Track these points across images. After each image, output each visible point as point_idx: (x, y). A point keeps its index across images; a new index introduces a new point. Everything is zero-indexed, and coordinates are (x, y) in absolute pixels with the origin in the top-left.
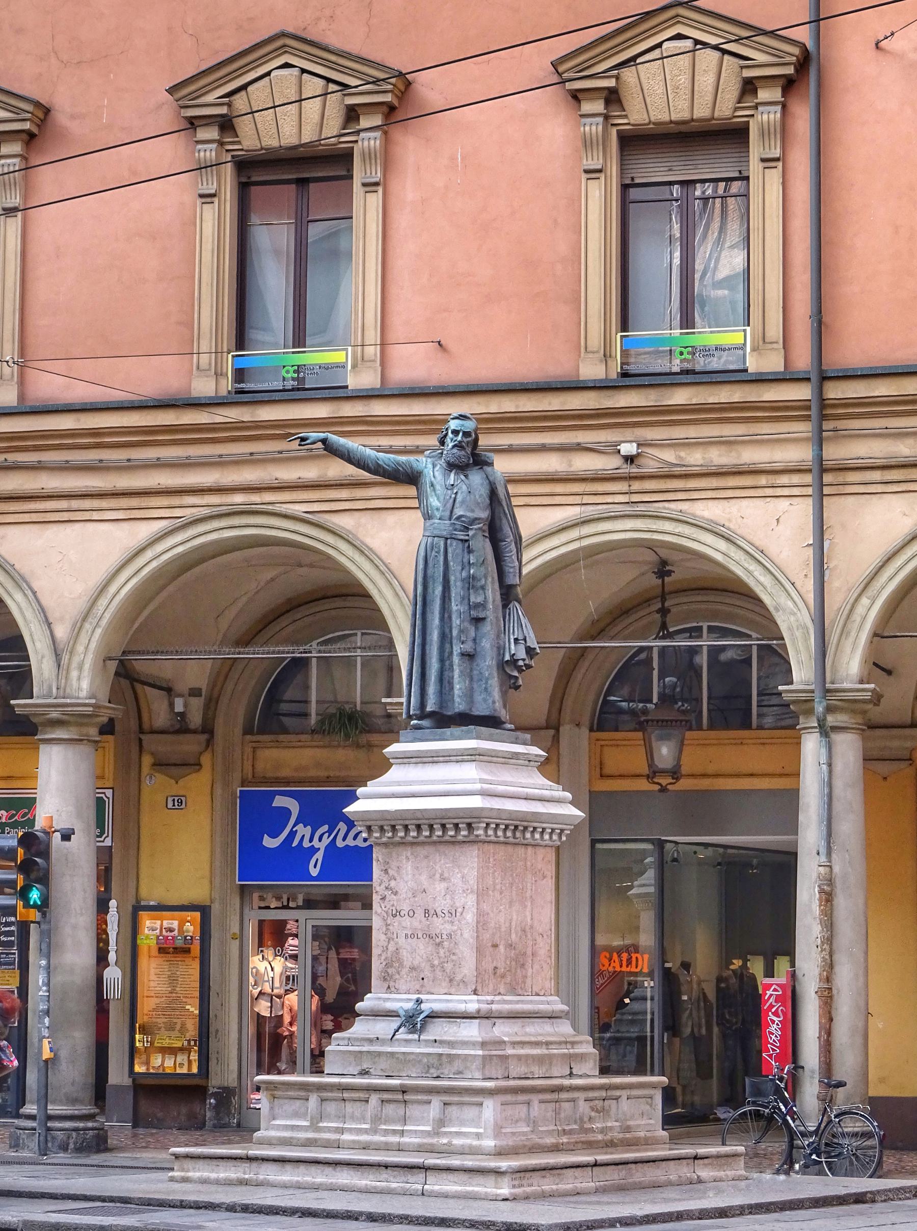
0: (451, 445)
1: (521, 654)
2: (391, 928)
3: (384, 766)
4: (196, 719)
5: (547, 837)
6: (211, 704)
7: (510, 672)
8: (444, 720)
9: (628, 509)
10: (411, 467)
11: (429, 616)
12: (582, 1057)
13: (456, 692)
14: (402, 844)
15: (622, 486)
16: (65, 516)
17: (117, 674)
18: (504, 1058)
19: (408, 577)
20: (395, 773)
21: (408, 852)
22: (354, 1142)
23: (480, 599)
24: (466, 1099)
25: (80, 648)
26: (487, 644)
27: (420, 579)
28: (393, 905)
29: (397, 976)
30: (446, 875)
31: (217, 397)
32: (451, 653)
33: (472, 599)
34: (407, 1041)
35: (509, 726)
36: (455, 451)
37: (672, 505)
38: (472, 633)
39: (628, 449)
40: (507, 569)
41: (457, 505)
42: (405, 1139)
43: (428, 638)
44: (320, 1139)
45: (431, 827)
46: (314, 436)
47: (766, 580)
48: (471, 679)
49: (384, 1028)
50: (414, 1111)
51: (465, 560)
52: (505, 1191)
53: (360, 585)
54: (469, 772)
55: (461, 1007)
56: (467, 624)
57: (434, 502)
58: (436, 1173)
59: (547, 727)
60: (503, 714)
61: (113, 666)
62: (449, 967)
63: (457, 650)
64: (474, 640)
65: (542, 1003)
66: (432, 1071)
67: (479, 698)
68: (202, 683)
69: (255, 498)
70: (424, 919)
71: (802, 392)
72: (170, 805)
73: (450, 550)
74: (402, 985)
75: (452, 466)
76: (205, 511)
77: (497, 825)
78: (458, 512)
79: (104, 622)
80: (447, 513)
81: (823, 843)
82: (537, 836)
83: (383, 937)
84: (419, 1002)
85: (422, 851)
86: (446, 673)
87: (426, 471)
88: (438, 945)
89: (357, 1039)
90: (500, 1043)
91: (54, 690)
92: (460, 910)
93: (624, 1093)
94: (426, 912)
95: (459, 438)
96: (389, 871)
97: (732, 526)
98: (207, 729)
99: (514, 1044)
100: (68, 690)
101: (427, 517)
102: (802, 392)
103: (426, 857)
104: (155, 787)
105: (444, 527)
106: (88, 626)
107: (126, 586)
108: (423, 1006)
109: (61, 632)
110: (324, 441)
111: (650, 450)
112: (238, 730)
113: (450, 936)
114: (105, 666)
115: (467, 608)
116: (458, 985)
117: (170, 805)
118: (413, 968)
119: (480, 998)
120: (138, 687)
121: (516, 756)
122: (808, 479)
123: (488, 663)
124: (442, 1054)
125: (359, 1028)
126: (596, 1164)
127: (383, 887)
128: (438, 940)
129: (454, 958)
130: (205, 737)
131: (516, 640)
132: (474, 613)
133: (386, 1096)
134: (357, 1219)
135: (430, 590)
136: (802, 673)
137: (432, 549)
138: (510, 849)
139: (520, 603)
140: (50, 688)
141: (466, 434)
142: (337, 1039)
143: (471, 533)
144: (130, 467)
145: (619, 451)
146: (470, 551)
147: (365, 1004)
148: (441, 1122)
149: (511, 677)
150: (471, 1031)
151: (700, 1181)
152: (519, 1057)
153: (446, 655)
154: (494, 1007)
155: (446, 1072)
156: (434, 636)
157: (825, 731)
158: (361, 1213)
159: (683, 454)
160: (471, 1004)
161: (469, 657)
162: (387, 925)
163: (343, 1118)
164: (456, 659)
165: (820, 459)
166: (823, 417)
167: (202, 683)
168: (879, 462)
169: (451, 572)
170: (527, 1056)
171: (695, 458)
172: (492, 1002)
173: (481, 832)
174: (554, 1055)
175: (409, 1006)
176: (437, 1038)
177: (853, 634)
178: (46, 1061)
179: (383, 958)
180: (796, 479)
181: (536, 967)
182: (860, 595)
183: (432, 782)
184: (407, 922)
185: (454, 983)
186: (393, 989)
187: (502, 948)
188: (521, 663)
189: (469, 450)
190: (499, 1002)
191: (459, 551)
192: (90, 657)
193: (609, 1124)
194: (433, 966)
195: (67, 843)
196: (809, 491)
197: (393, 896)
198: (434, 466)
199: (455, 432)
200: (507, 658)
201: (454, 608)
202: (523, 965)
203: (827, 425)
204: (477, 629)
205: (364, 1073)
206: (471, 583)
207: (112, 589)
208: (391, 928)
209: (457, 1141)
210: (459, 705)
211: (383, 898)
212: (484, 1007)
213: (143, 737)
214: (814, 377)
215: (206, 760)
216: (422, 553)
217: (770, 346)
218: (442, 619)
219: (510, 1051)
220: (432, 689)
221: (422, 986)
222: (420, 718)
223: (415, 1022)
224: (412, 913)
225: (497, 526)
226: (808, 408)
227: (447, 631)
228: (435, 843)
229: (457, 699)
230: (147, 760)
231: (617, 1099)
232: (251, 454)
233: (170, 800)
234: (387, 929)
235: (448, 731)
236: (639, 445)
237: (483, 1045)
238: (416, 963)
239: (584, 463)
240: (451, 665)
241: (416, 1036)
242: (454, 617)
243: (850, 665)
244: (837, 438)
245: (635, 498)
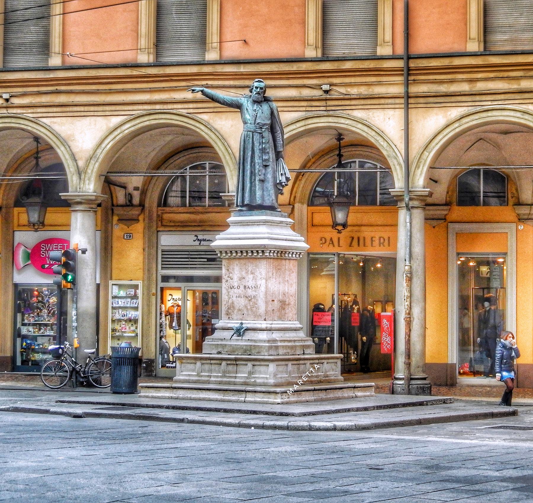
0: (255, 93)
1: (284, 180)
3: (227, 226)
4: (136, 200)
5: (294, 256)
6: (144, 193)
7: (278, 187)
8: (252, 208)
9: (325, 113)
10: (238, 102)
11: (246, 164)
12: (308, 347)
13: (257, 196)
14: (235, 258)
15: (323, 103)
16: (83, 114)
17: (104, 181)
18: (277, 347)
19: (235, 145)
20: (231, 230)
21: (237, 262)
22: (215, 381)
23: (267, 157)
24: (262, 363)
25: (89, 171)
26: (270, 176)
27: (242, 149)
30: (253, 272)
31: (148, 63)
32: (255, 179)
33: (264, 158)
34: (238, 340)
35: (279, 210)
36: (256, 95)
37: (345, 112)
38: (264, 171)
39: (326, 87)
40: (278, 145)
41: (257, 118)
42: (237, 380)
43: (245, 174)
45: (247, 252)
46: (198, 89)
47: (385, 145)
48: (263, 191)
49: (227, 334)
50: (241, 368)
51: (261, 141)
52: (279, 401)
53: (207, 142)
54: (263, 229)
55: (259, 326)
56: (261, 168)
57: (248, 117)
59: (289, 204)
60: (276, 205)
61: (103, 178)
62: (254, 309)
63: (257, 178)
64: (264, 175)
65: (292, 324)
66: (248, 352)
67: (266, 198)
68: (140, 185)
69: (165, 107)
70: (244, 290)
71: (400, 64)
72: (125, 238)
73: (255, 137)
74: (234, 316)
75: (255, 102)
76: (144, 112)
77: (274, 251)
78: (258, 121)
79: (100, 160)
80: (253, 122)
81: (407, 256)
82: (290, 255)
83: (227, 297)
84: (242, 324)
86: (253, 188)
87: (244, 104)
89: (216, 339)
90: (275, 341)
91: (78, 189)
92: (259, 286)
93: (325, 361)
94: (245, 287)
95: (258, 90)
97: (370, 121)
98: (142, 205)
99: (281, 341)
100: (84, 189)
101: (245, 123)
102: (400, 64)
103: (245, 264)
104: (118, 230)
105: (252, 127)
106: (92, 162)
107: (108, 144)
108: (244, 325)
109: (81, 163)
110: (202, 91)
111: (334, 88)
112: (155, 204)
113: (254, 297)
114: (100, 178)
115: (261, 161)
117: (125, 238)
118: (239, 310)
119: (267, 322)
120: (112, 187)
121: (281, 222)
122: (402, 101)
123: (270, 185)
125: (217, 334)
126: (315, 390)
130: (141, 208)
131: (282, 174)
132: (265, 163)
133: (229, 362)
135: (246, 153)
136: (399, 184)
137: (247, 136)
138: (279, 260)
139: (283, 159)
140: (76, 188)
141: (261, 88)
142: (207, 339)
143: (263, 130)
144: (110, 92)
145: (322, 88)
146: (263, 137)
147: (219, 323)
148: (250, 373)
149: (279, 189)
150: (263, 336)
151: (356, 397)
152: (283, 346)
153: (253, 180)
154: (273, 326)
155: (253, 352)
156: (248, 173)
157: (409, 208)
158: (221, 409)
159: (349, 90)
160: (264, 325)
161: (262, 181)
164: (257, 183)
165: (407, 92)
166: (409, 75)
167: (140, 185)
168: (432, 94)
169: (255, 146)
170: (286, 346)
171: (354, 91)
172: (272, 324)
173: (268, 254)
174: (297, 346)
175: (237, 325)
177: (421, 167)
178: (76, 348)
180: (398, 101)
181: (290, 309)
182: (424, 151)
184: (236, 290)
185: (257, 316)
187: (276, 301)
188: (283, 184)
189: (262, 95)
190: (275, 324)
191: (258, 137)
192: (94, 174)
193: (319, 374)
194: (247, 309)
195: (84, 255)
196: (403, 106)
198: (248, 101)
199: (257, 88)
200: (278, 182)
201: (257, 161)
202: (284, 309)
203: (411, 78)
204: (265, 170)
205: (219, 353)
206: (263, 151)
207: (103, 145)
209: (258, 381)
210: (259, 201)
211: (227, 281)
212: (269, 326)
213: (113, 208)
214: (405, 58)
215: (141, 218)
216: (243, 138)
217: (387, 44)
218: (251, 166)
219: (279, 344)
220: (247, 195)
222: (242, 206)
223: (240, 332)
225: (274, 126)
226: (403, 71)
227: (253, 170)
228: (248, 258)
229: (258, 199)
230: (115, 218)
231: (322, 363)
232: (164, 88)
233: (125, 235)
235: (254, 212)
236: (330, 85)
237: (269, 341)
238: (240, 308)
239: (306, 93)
240: (255, 185)
241: (240, 338)
242: (256, 165)
243: (420, 181)
244: (414, 83)
245: (328, 108)
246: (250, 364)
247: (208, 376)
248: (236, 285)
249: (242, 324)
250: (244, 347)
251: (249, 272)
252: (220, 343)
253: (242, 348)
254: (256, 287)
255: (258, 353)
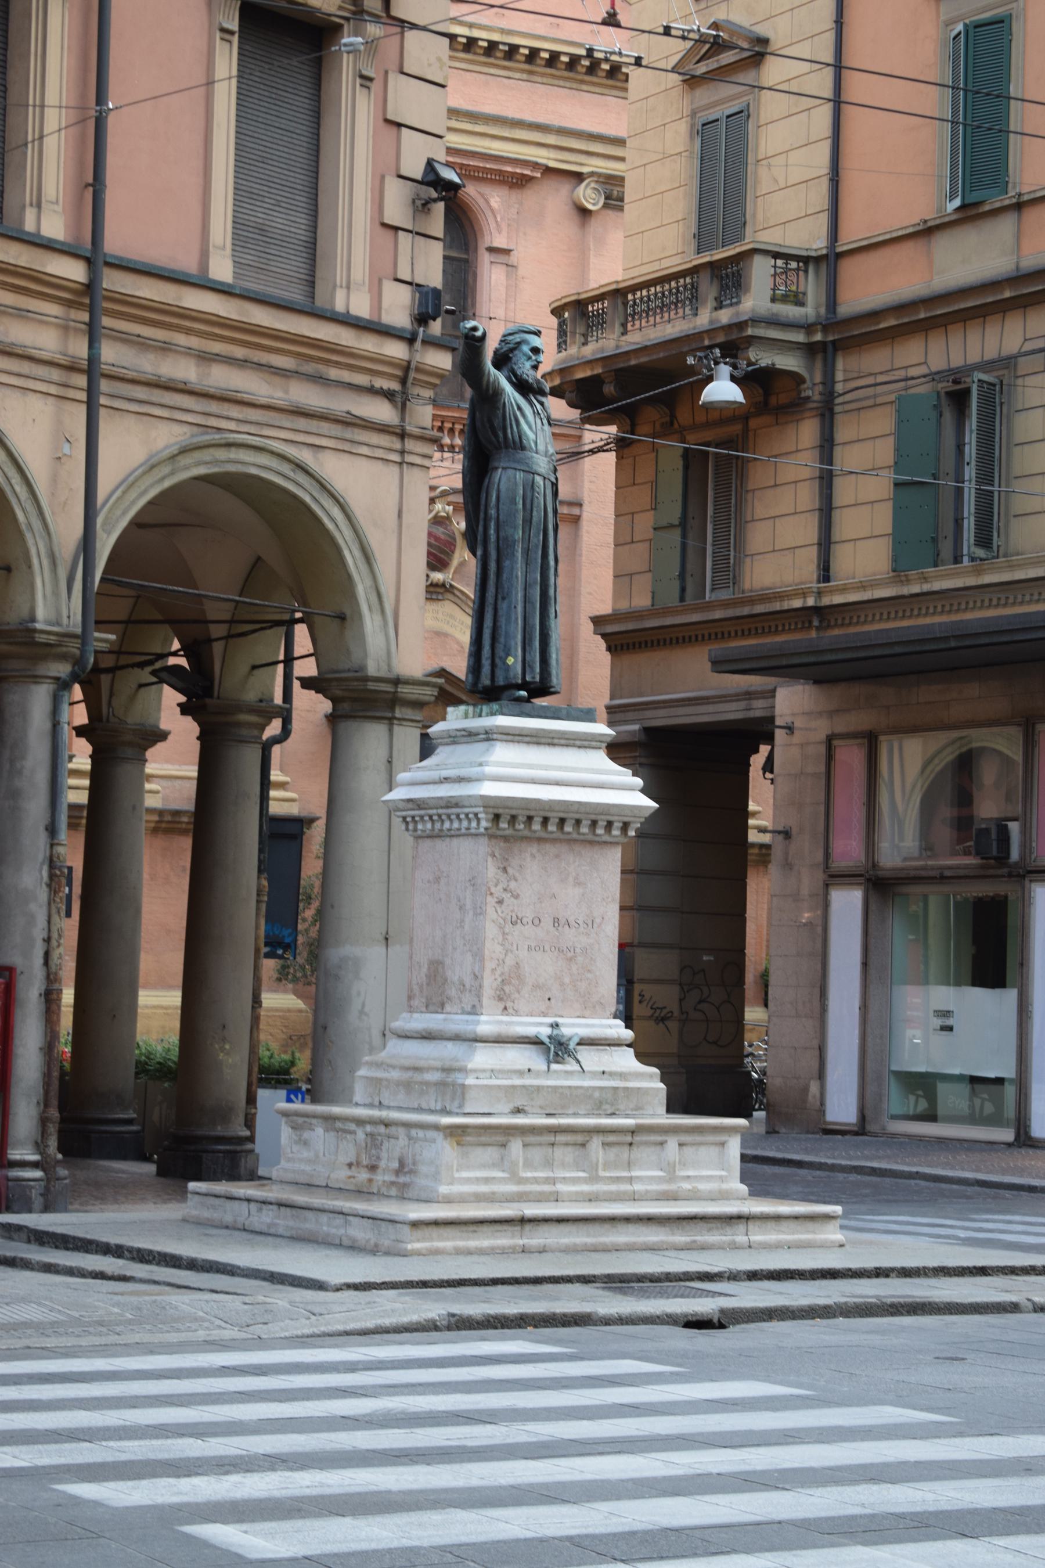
2: (509, 937)
21: (533, 848)
22: (577, 1193)
28: (512, 911)
29: (517, 995)
42: (638, 1187)
44: (530, 1192)
58: (758, 1223)
66: (607, 1107)
70: (552, 929)
85: (551, 849)
88: (570, 959)
92: (598, 921)
94: (556, 921)
96: (509, 870)
103: (557, 856)
116: (594, 1007)
118: (537, 987)
124: (617, 1088)
127: (500, 887)
128: (569, 955)
129: (589, 975)
134: (887, 1276)
155: (622, 1107)
158: (892, 1270)
162: (504, 934)
163: (549, 1164)
176: (606, 1069)
179: (498, 972)
183: (546, 768)
184: (528, 930)
186: (510, 1011)
194: (562, 984)
197: (512, 899)
205: (518, 1111)
208: (509, 937)
209: (703, 1186)
211: (500, 902)
221: (549, 1008)
224: (537, 921)
234: (504, 939)
246: (672, 1143)
247: (548, 1180)
248: (528, 914)
249: (555, 1026)
250: (597, 1094)
251: (571, 879)
252: (518, 1082)
253: (591, 1097)
254: (591, 923)
255: (638, 1108)
